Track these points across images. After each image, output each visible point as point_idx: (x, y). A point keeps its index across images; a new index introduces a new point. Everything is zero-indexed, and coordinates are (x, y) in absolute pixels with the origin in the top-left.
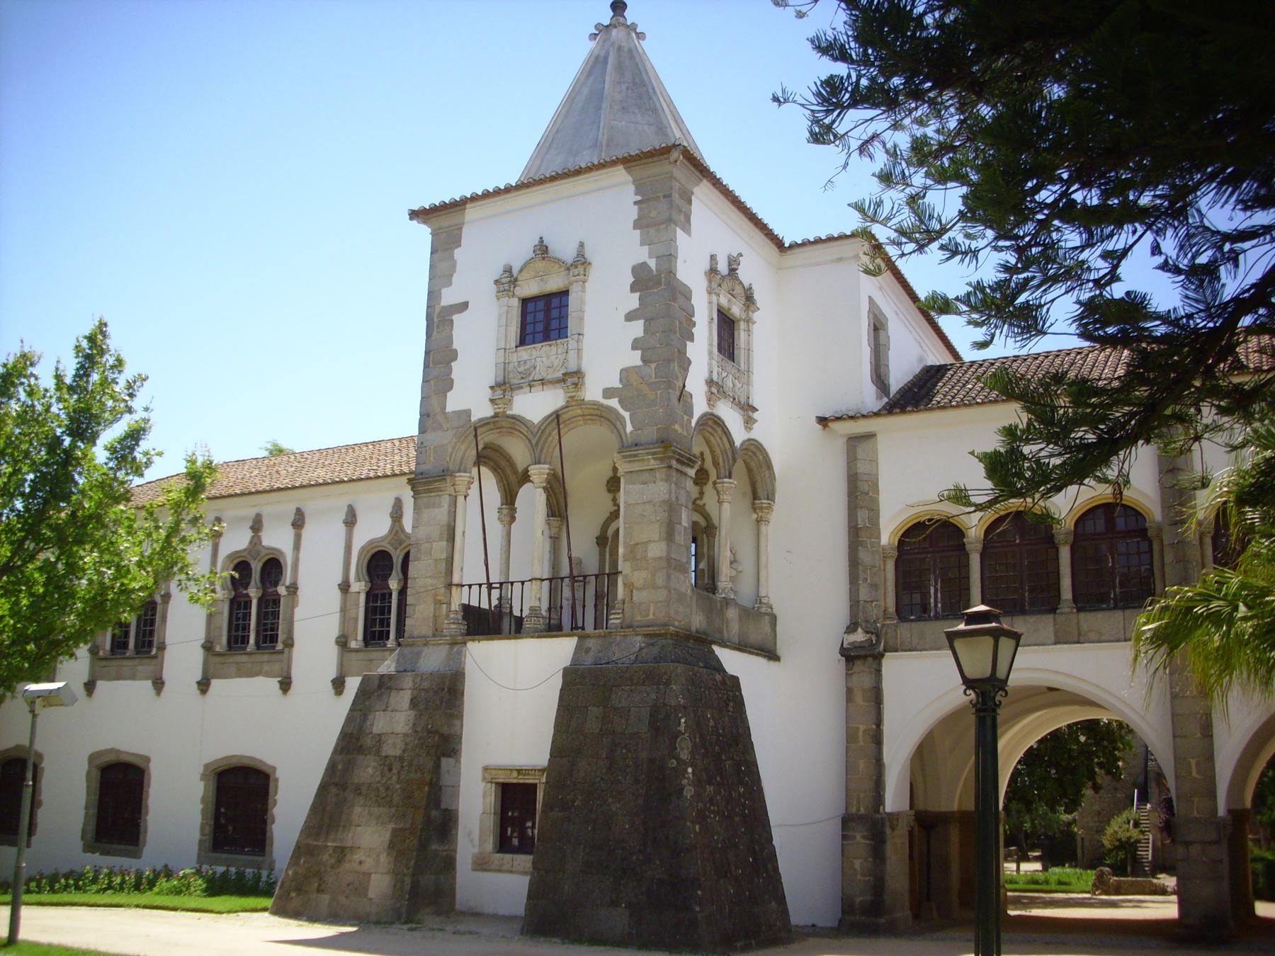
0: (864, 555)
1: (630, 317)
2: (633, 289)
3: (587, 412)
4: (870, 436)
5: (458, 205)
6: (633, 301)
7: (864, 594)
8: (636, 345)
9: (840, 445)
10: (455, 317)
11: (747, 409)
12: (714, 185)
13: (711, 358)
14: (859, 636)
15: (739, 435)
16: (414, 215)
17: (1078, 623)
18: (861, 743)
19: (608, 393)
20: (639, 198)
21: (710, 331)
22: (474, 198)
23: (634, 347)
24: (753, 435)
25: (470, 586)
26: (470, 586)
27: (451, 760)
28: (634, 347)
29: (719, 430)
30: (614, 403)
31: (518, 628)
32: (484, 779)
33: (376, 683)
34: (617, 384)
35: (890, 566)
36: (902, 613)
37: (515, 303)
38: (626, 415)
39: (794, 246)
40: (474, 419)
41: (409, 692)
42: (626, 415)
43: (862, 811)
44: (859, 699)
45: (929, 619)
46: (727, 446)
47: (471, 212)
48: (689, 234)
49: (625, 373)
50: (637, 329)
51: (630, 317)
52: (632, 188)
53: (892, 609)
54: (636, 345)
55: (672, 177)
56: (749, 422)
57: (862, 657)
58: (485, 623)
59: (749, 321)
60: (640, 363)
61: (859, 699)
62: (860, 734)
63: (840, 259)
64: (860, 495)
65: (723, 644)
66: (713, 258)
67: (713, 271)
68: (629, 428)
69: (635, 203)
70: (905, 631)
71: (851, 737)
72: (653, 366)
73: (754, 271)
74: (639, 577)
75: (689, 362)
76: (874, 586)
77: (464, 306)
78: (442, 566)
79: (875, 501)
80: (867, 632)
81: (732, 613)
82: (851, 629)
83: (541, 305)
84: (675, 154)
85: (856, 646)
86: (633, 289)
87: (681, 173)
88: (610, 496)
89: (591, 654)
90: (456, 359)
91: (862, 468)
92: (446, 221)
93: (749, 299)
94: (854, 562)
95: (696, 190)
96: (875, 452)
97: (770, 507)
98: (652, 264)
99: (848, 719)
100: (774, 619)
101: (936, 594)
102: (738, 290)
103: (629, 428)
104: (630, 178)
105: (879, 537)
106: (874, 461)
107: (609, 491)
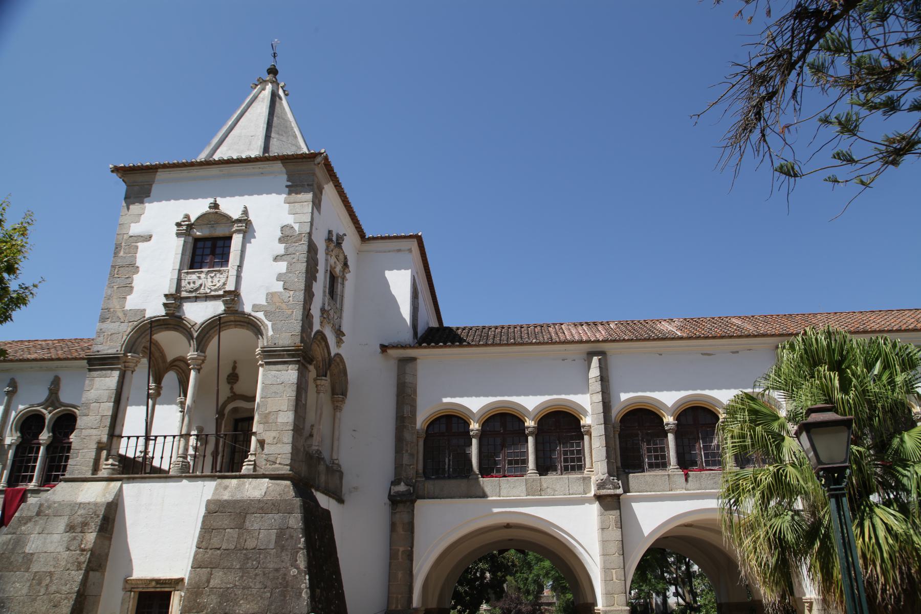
0: (407, 436)
1: (277, 258)
2: (281, 240)
3: (238, 319)
4: (413, 359)
6: (280, 249)
7: (406, 460)
8: (279, 277)
9: (393, 365)
10: (141, 245)
11: (339, 333)
12: (335, 186)
13: (324, 295)
14: (402, 488)
15: (334, 350)
16: (116, 170)
17: (541, 483)
18: (400, 560)
19: (256, 308)
20: (289, 183)
21: (325, 277)
23: (278, 279)
24: (340, 351)
25: (129, 438)
26: (129, 438)
27: (98, 574)
28: (278, 279)
29: (323, 343)
30: (260, 315)
31: (159, 474)
32: (124, 589)
33: (36, 509)
34: (263, 302)
35: (421, 443)
36: (426, 475)
37: (190, 239)
38: (269, 324)
39: (369, 239)
40: (147, 316)
41: (66, 518)
42: (269, 324)
43: (400, 607)
44: (400, 530)
45: (444, 478)
46: (327, 355)
47: (161, 175)
48: (320, 213)
49: (271, 296)
50: (282, 266)
51: (277, 258)
52: (286, 176)
53: (421, 471)
54: (279, 277)
55: (314, 174)
56: (339, 342)
57: (401, 503)
58: (136, 469)
59: (344, 278)
60: (281, 290)
61: (400, 530)
62: (400, 553)
63: (399, 251)
64: (405, 396)
65: (317, 490)
66: (330, 232)
67: (329, 240)
68: (270, 333)
69: (287, 186)
70: (430, 486)
71: (393, 555)
72: (292, 293)
73: (350, 244)
74: (268, 437)
75: (314, 295)
76: (412, 455)
77: (148, 238)
78: (108, 422)
79: (414, 400)
80: (407, 485)
81: (322, 468)
82: (395, 483)
83: (209, 244)
84: (319, 159)
85: (399, 494)
86: (281, 240)
87: (320, 173)
88: (229, 386)
89: (229, 489)
90: (137, 272)
91: (408, 379)
92: (140, 178)
93: (346, 265)
94: (399, 440)
95: (326, 186)
96: (416, 370)
97: (343, 401)
98: (296, 227)
99: (391, 543)
100: (341, 474)
101: (449, 465)
102: (341, 257)
103: (270, 333)
104: (284, 170)
105: (415, 424)
106: (415, 375)
107: (229, 383)
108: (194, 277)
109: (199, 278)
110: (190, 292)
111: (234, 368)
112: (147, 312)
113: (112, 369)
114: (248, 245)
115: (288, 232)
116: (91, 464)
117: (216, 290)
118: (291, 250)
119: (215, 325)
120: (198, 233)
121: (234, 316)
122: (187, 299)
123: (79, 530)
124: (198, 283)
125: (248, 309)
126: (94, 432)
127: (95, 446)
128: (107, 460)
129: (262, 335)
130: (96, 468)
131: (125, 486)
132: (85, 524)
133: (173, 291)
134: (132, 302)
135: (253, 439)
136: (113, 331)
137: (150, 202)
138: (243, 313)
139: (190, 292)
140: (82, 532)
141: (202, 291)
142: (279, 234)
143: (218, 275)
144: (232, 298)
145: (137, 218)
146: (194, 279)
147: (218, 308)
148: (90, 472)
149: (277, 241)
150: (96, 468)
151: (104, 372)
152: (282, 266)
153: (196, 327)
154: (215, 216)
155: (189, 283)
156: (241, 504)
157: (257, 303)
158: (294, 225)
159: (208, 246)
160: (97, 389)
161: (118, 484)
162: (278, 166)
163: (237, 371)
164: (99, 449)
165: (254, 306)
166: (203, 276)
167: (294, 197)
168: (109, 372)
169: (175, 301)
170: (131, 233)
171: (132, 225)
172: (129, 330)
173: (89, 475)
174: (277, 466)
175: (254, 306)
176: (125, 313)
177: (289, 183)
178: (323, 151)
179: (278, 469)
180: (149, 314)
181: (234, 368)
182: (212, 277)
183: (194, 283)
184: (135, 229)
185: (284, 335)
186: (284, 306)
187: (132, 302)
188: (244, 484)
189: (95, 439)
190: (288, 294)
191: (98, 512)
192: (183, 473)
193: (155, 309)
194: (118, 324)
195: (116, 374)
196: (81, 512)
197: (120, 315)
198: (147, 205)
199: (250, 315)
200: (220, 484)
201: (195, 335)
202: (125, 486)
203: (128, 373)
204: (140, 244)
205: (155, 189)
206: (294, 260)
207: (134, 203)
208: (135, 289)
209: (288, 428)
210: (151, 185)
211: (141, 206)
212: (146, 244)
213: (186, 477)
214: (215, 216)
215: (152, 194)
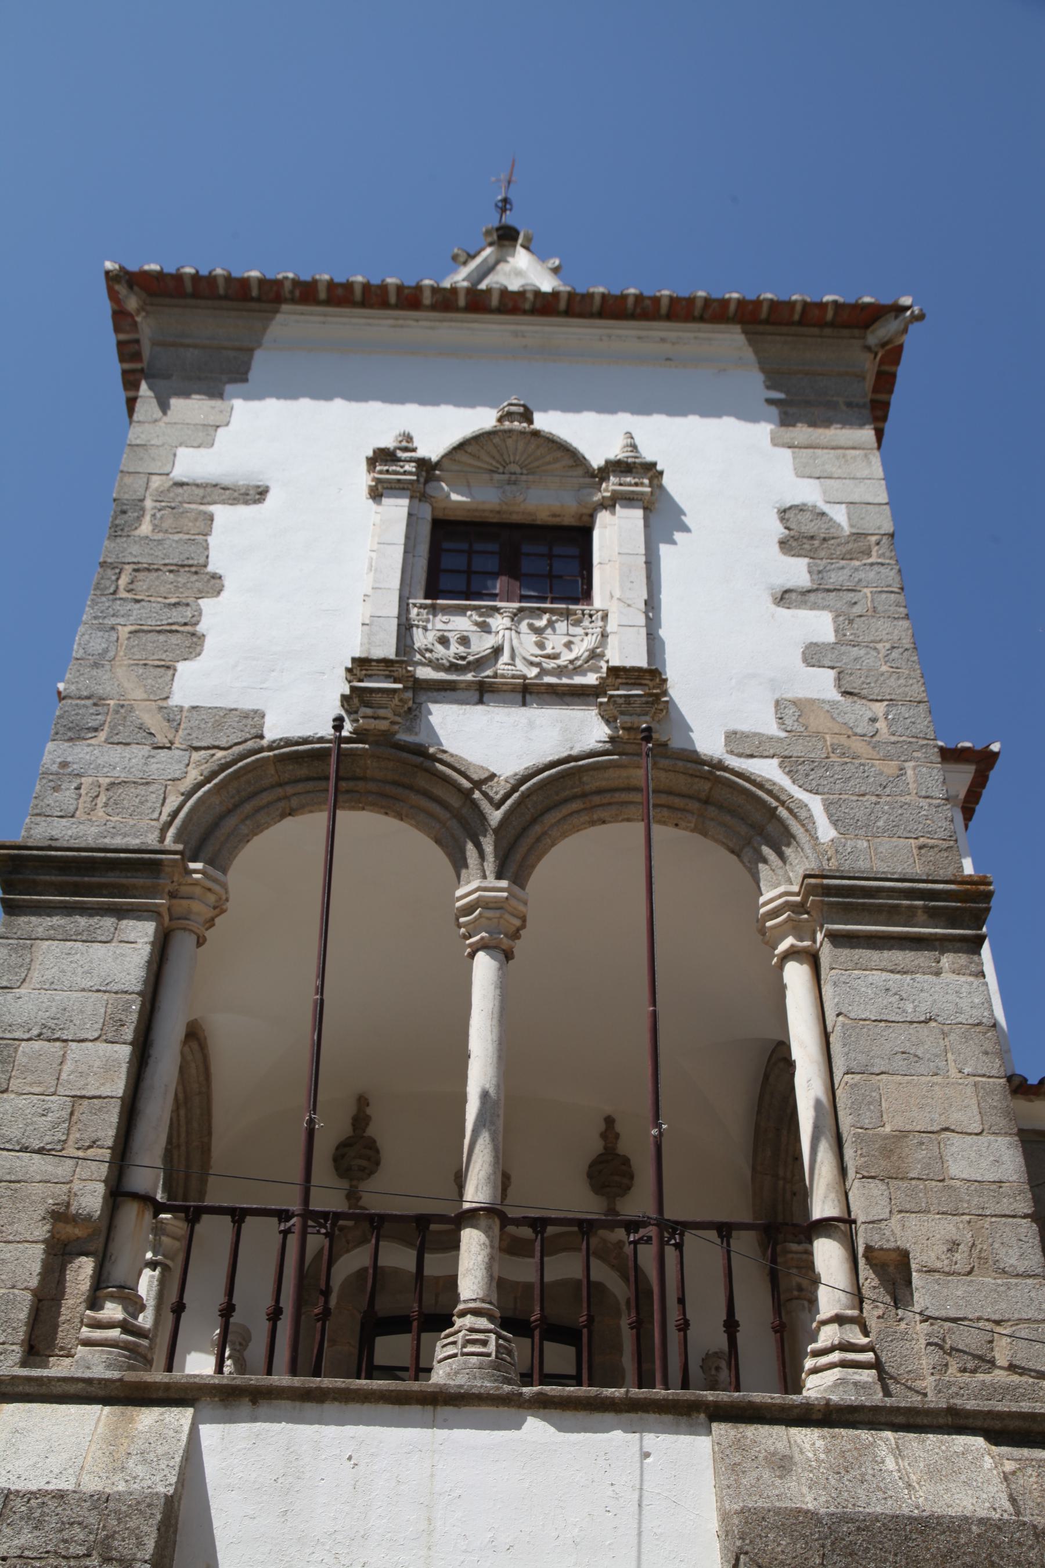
8: (814, 655)
10: (221, 512)
22: (306, 293)
30: (768, 769)
38: (815, 804)
40: (273, 731)
47: (290, 322)
49: (792, 710)
52: (757, 379)
54: (814, 655)
68: (826, 832)
69: (770, 402)
72: (879, 708)
78: (106, 1126)
86: (785, 545)
88: (345, 1184)
98: (839, 515)
103: (826, 832)
104: (749, 354)
108: (462, 624)
110: (453, 668)
111: (360, 1120)
112: (269, 721)
113: (121, 913)
114: (664, 549)
115: (810, 527)
116: (22, 1314)
117: (560, 671)
118: (834, 579)
119: (559, 795)
120: (455, 497)
121: (650, 771)
122: (444, 691)
124: (482, 645)
125: (708, 742)
127: (42, 1231)
128: (94, 1303)
129: (789, 837)
130: (39, 1342)
131: (208, 1432)
134: (194, 684)
135: (828, 1256)
136: (119, 774)
137: (247, 397)
138: (693, 758)
139: (453, 668)
141: (502, 664)
142: (778, 530)
143: (561, 626)
144: (638, 696)
145: (205, 435)
146: (453, 631)
148: (17, 1352)
149: (776, 548)
150: (39, 1342)
151: (82, 921)
152: (819, 625)
153: (498, 790)
154: (514, 449)
155: (444, 641)
156: (942, 1542)
157: (744, 727)
159: (500, 541)
160: (51, 986)
161: (182, 1417)
162: (732, 339)
163: (372, 1131)
164: (59, 1254)
165: (732, 737)
166: (499, 622)
167: (802, 433)
168: (108, 922)
169: (387, 693)
170: (180, 472)
171: (181, 451)
172: (194, 775)
174: (1000, 1376)
175: (732, 737)
176: (173, 718)
178: (906, 301)
179: (1007, 1390)
181: (360, 1120)
182: (538, 631)
184: (191, 464)
185: (886, 845)
186: (858, 746)
187: (194, 684)
188: (863, 1450)
189: (50, 1196)
190: (859, 712)
191: (122, 1547)
192: (526, 1379)
193: (304, 707)
194: (139, 752)
195: (141, 934)
197: (153, 721)
198: (238, 404)
199: (720, 766)
200: (739, 1445)
201: (495, 816)
202: (208, 1432)
203: (183, 944)
204: (217, 510)
205: (261, 362)
206: (857, 610)
207: (186, 394)
208: (208, 643)
209: (1006, 1206)
210: (250, 351)
211: (217, 403)
213: (542, 1405)
214: (514, 449)
215: (251, 375)
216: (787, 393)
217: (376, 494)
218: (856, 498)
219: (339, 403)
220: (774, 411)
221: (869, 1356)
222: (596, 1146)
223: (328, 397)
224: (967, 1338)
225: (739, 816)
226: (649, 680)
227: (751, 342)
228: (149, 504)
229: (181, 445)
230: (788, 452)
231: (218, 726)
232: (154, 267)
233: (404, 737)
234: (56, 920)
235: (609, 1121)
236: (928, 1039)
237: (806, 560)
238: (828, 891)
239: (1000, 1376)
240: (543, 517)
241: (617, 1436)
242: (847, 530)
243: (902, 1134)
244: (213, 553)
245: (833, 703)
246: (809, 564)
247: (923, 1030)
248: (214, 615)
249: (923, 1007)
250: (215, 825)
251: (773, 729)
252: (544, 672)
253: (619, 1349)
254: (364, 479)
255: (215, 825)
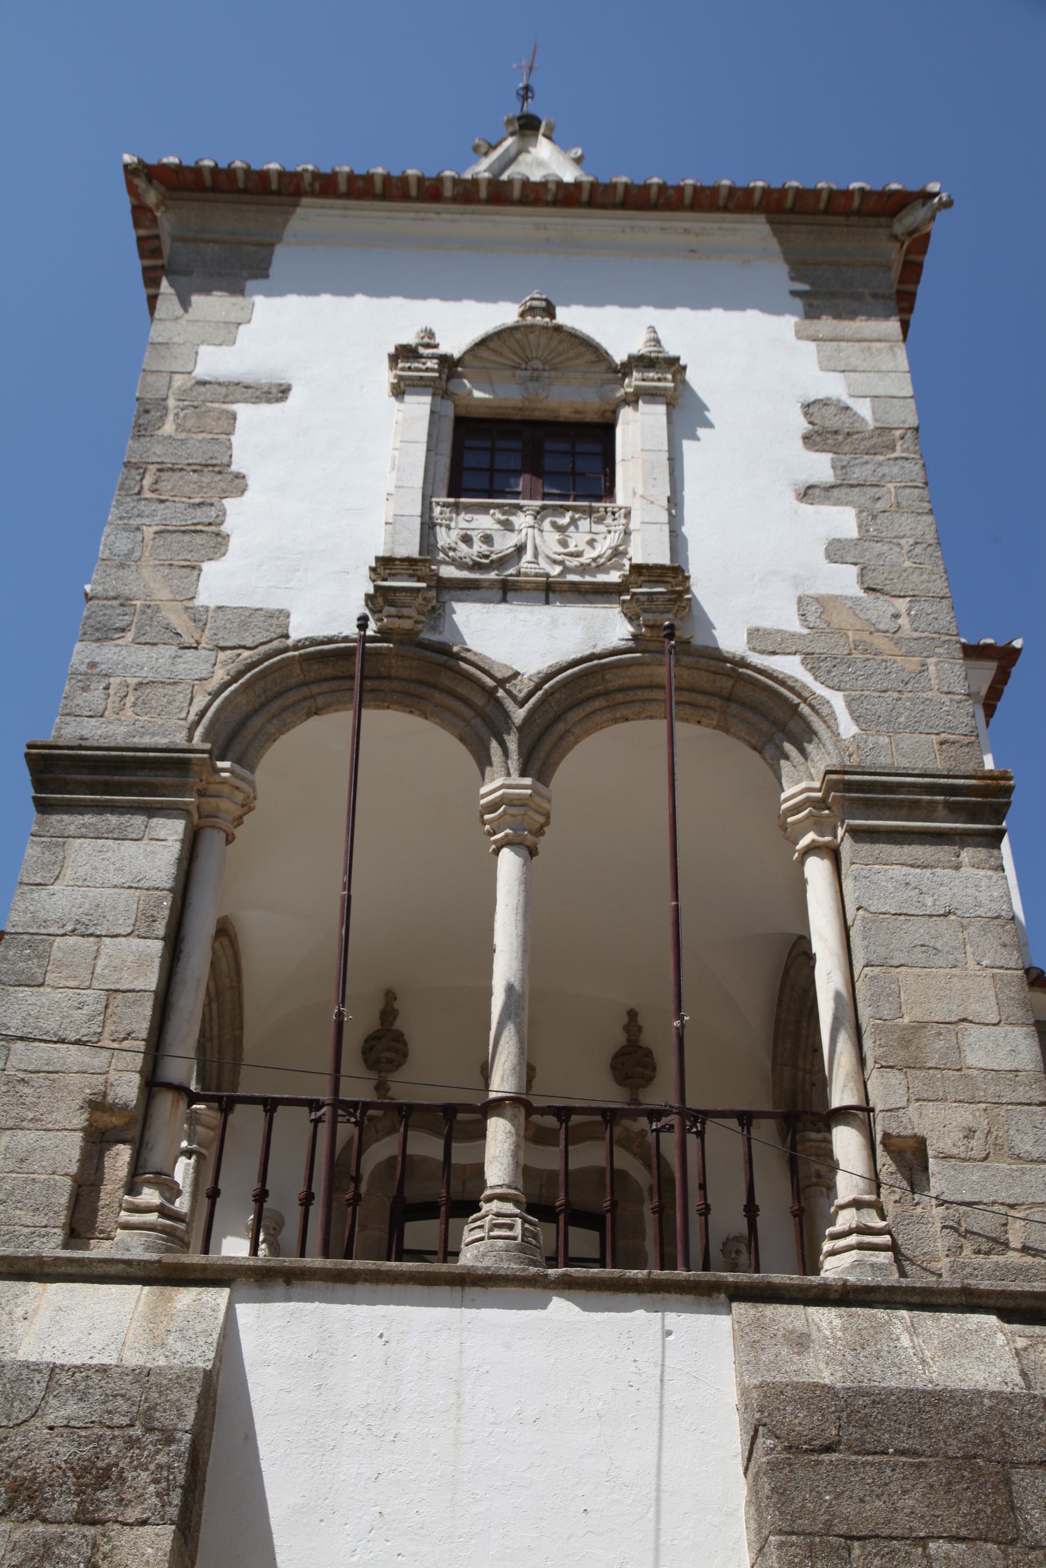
5: (286, 191)
8: (837, 551)
10: (242, 410)
20: (804, 287)
22: (326, 186)
38: (837, 701)
40: (296, 634)
47: (310, 216)
50: (842, 521)
52: (781, 270)
54: (837, 551)
60: (855, 590)
68: (848, 728)
69: (795, 293)
72: (902, 604)
78: (140, 1018)
88: (374, 1075)
92: (227, 219)
98: (864, 409)
103: (848, 728)
104: (774, 244)
108: (485, 522)
109: (507, 526)
110: (476, 566)
111: (388, 1014)
112: (294, 621)
113: (151, 811)
114: (687, 445)
116: (63, 1199)
117: (583, 569)
118: (858, 474)
119: (583, 692)
120: (477, 394)
121: (673, 668)
122: (468, 589)
123: (66, 1505)
124: (505, 543)
125: (731, 640)
126: (75, 1056)
127: (80, 1119)
128: (132, 1189)
129: (811, 733)
130: (80, 1225)
131: (245, 1312)
132: (95, 1478)
133: (410, 548)
134: (220, 584)
135: (846, 1143)
136: (147, 674)
137: (269, 293)
138: (716, 655)
139: (476, 566)
140: (84, 1518)
142: (802, 425)
143: (584, 524)
144: (661, 594)
145: (227, 332)
146: (477, 529)
147: (606, 628)
148: (58, 1235)
149: (800, 443)
150: (80, 1225)
151: (113, 819)
152: (842, 521)
153: (521, 688)
154: (537, 345)
155: (467, 540)
156: (956, 1414)
157: (767, 624)
158: (850, 402)
159: (522, 437)
160: (83, 883)
161: (222, 1295)
162: (756, 229)
163: (399, 1024)
164: (97, 1141)
165: (755, 634)
166: (522, 521)
167: (826, 325)
168: (139, 820)
169: (411, 592)
170: (201, 371)
171: (204, 350)
172: (220, 675)
173: (51, 1246)
174: (1014, 1257)
175: (755, 634)
176: (199, 618)
177: (804, 287)
178: (934, 187)
179: (1021, 1271)
180: (303, 627)
181: (388, 1014)
182: (561, 529)
183: (487, 539)
184: (213, 362)
185: (907, 740)
186: (880, 642)
187: (220, 584)
188: (880, 1327)
189: (85, 1087)
190: (881, 609)
191: (164, 1418)
192: (552, 1261)
193: (329, 607)
195: (171, 832)
196: (64, 1410)
197: (179, 621)
199: (742, 663)
200: (758, 1324)
201: (519, 714)
203: (212, 842)
204: (240, 408)
205: (282, 257)
206: (880, 505)
207: (207, 291)
209: (1022, 1094)
210: (272, 245)
211: (238, 300)
212: (266, 410)
213: (567, 1286)
214: (537, 345)
215: (273, 270)
216: (812, 284)
217: (399, 391)
218: (881, 392)
219: (360, 299)
220: (798, 303)
221: (886, 1239)
222: (618, 1039)
223: (349, 293)
224: (983, 1222)
225: (760, 712)
226: (672, 577)
227: (776, 232)
228: (171, 403)
229: (203, 343)
230: (812, 346)
231: (244, 625)
232: (173, 160)
233: (428, 636)
234: (88, 819)
235: (632, 1014)
236: (947, 932)
237: (830, 455)
238: (849, 786)
239: (1014, 1257)
240: (566, 413)
241: (640, 1315)
242: (871, 424)
243: (921, 1025)
244: (235, 452)
245: (855, 600)
246: (833, 459)
247: (942, 923)
248: (238, 514)
249: (943, 901)
250: (242, 724)
251: (794, 625)
252: (567, 570)
253: (641, 1233)
254: (386, 377)
255: (242, 724)
